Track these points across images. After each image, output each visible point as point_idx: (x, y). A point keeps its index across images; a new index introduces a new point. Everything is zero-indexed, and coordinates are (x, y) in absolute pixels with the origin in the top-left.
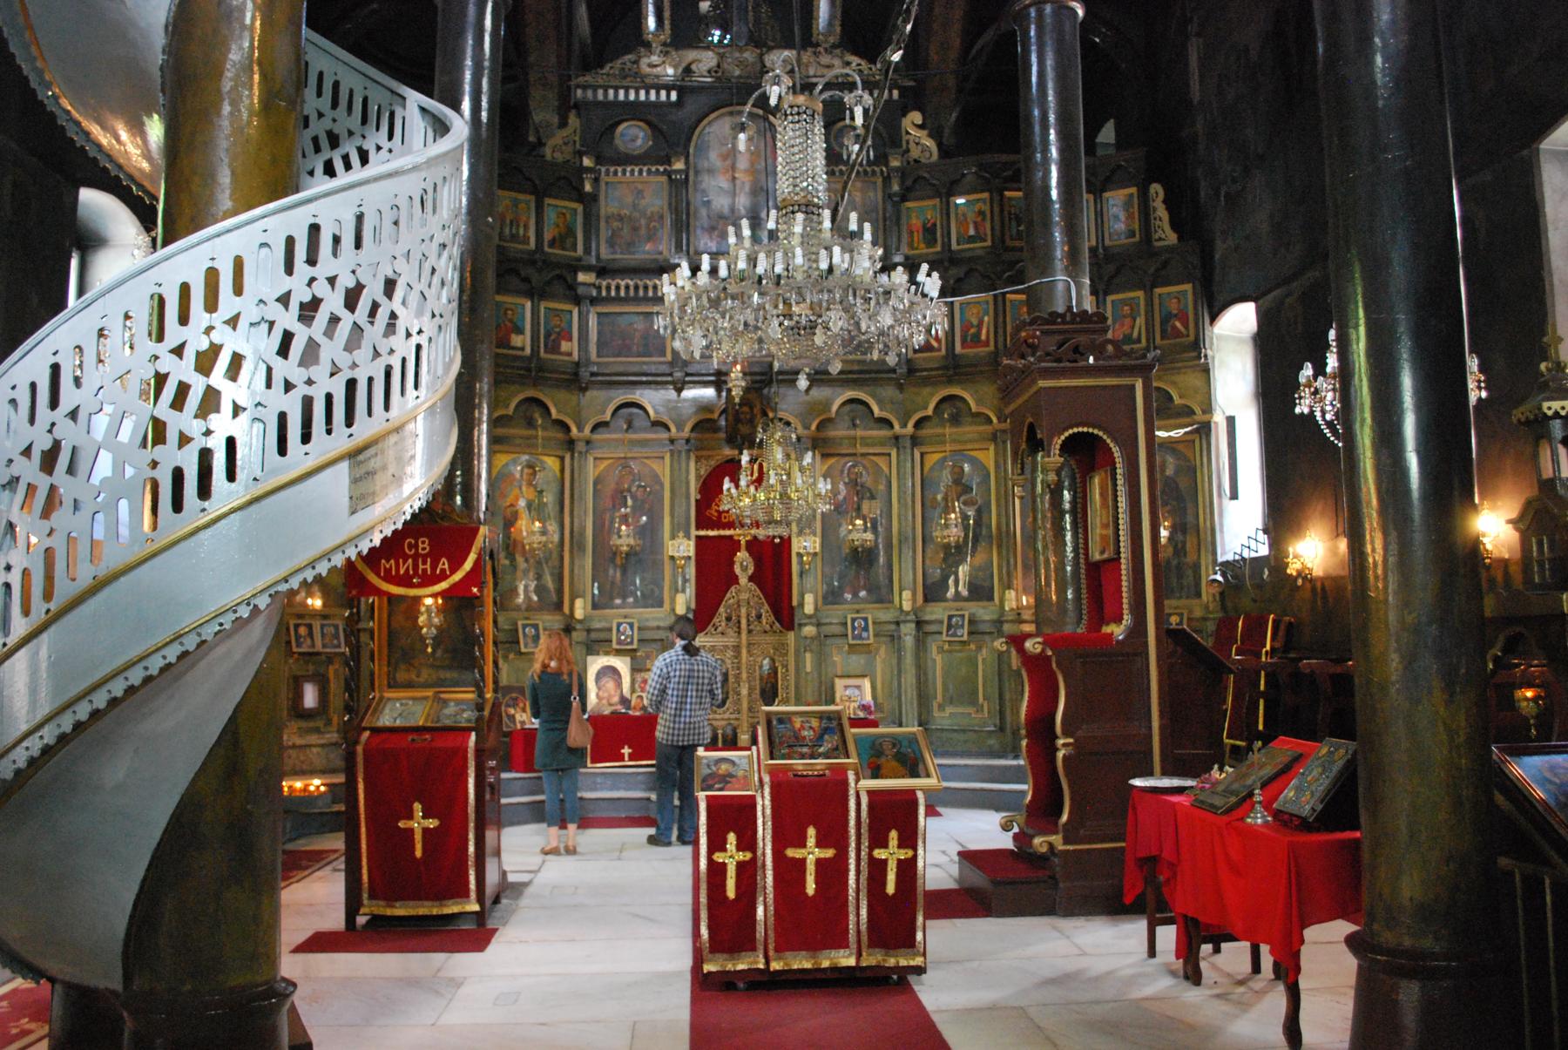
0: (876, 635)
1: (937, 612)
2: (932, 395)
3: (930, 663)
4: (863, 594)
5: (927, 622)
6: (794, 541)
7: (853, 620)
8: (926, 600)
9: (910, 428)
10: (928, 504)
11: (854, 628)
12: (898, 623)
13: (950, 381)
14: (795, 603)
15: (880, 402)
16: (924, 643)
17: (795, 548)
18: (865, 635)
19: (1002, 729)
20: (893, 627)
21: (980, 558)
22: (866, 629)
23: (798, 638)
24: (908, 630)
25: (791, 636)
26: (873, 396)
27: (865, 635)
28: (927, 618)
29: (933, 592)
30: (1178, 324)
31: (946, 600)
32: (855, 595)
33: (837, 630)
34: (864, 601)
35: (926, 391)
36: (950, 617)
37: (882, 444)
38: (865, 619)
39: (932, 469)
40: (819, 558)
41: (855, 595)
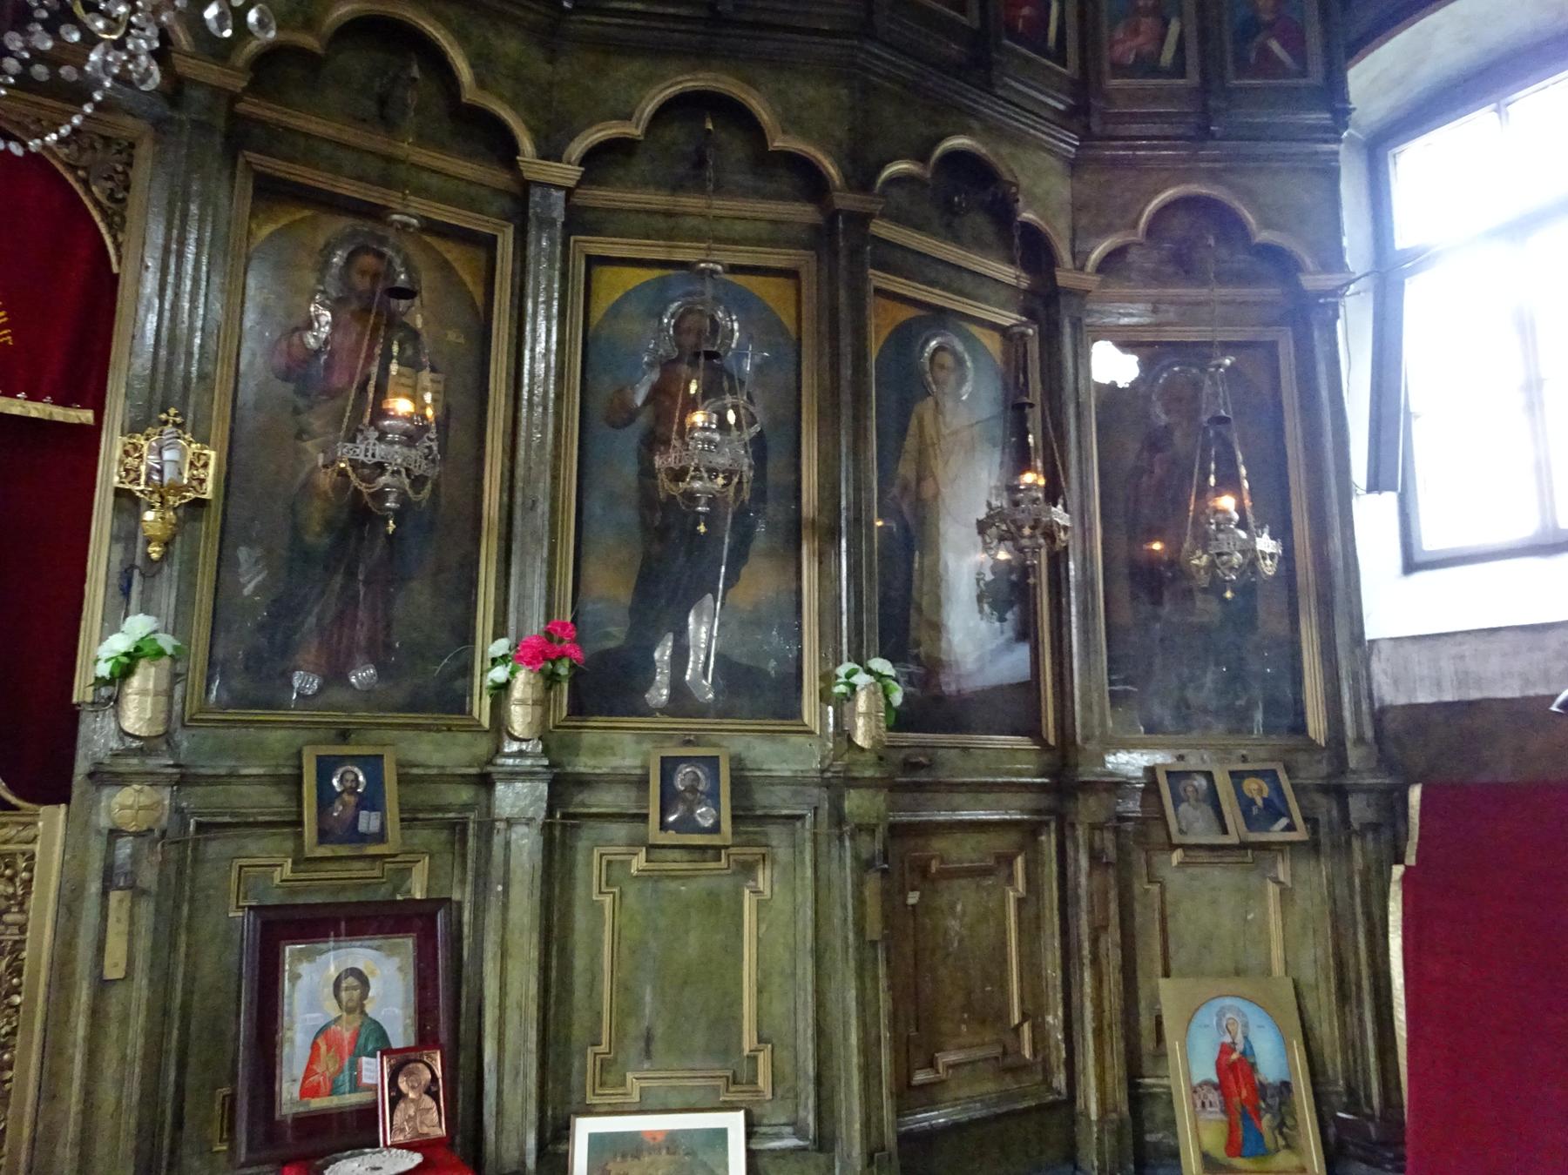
0: (409, 820)
1: (618, 749)
2: (648, 81)
3: (581, 920)
4: (363, 675)
5: (584, 782)
6: (112, 446)
7: (326, 767)
8: (579, 708)
9: (567, 172)
10: (598, 407)
11: (326, 797)
12: (485, 781)
13: (702, 56)
14: (82, 692)
15: (480, 61)
16: (568, 848)
17: (109, 475)
18: (368, 822)
19: (824, 1142)
20: (465, 794)
21: (759, 582)
22: (373, 800)
23: (78, 828)
24: (519, 800)
25: (52, 820)
26: (462, 38)
27: (368, 822)
28: (584, 765)
29: (597, 684)
30: (1275, 46)
31: (648, 712)
32: (335, 675)
33: (268, 801)
34: (368, 697)
35: (627, 69)
36: (669, 766)
37: (471, 204)
38: (372, 765)
39: (615, 310)
40: (209, 527)
41: (335, 675)
